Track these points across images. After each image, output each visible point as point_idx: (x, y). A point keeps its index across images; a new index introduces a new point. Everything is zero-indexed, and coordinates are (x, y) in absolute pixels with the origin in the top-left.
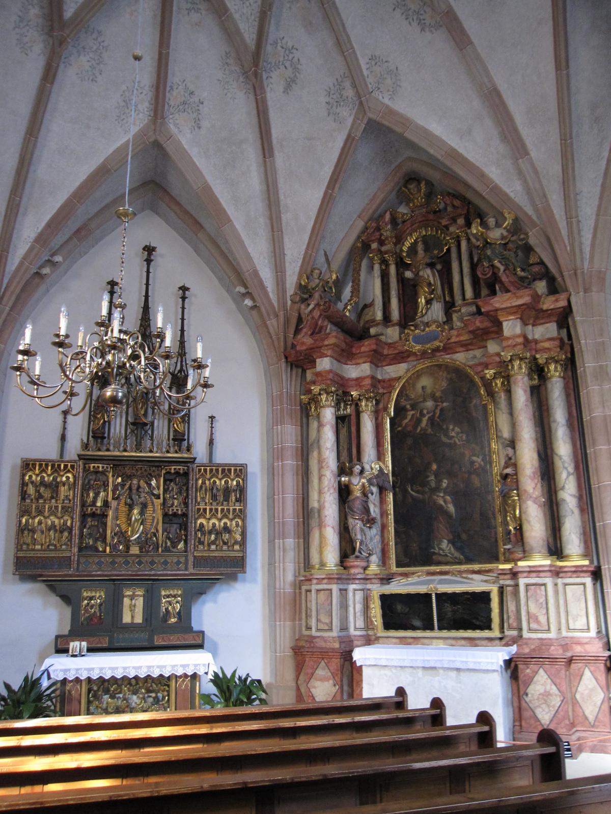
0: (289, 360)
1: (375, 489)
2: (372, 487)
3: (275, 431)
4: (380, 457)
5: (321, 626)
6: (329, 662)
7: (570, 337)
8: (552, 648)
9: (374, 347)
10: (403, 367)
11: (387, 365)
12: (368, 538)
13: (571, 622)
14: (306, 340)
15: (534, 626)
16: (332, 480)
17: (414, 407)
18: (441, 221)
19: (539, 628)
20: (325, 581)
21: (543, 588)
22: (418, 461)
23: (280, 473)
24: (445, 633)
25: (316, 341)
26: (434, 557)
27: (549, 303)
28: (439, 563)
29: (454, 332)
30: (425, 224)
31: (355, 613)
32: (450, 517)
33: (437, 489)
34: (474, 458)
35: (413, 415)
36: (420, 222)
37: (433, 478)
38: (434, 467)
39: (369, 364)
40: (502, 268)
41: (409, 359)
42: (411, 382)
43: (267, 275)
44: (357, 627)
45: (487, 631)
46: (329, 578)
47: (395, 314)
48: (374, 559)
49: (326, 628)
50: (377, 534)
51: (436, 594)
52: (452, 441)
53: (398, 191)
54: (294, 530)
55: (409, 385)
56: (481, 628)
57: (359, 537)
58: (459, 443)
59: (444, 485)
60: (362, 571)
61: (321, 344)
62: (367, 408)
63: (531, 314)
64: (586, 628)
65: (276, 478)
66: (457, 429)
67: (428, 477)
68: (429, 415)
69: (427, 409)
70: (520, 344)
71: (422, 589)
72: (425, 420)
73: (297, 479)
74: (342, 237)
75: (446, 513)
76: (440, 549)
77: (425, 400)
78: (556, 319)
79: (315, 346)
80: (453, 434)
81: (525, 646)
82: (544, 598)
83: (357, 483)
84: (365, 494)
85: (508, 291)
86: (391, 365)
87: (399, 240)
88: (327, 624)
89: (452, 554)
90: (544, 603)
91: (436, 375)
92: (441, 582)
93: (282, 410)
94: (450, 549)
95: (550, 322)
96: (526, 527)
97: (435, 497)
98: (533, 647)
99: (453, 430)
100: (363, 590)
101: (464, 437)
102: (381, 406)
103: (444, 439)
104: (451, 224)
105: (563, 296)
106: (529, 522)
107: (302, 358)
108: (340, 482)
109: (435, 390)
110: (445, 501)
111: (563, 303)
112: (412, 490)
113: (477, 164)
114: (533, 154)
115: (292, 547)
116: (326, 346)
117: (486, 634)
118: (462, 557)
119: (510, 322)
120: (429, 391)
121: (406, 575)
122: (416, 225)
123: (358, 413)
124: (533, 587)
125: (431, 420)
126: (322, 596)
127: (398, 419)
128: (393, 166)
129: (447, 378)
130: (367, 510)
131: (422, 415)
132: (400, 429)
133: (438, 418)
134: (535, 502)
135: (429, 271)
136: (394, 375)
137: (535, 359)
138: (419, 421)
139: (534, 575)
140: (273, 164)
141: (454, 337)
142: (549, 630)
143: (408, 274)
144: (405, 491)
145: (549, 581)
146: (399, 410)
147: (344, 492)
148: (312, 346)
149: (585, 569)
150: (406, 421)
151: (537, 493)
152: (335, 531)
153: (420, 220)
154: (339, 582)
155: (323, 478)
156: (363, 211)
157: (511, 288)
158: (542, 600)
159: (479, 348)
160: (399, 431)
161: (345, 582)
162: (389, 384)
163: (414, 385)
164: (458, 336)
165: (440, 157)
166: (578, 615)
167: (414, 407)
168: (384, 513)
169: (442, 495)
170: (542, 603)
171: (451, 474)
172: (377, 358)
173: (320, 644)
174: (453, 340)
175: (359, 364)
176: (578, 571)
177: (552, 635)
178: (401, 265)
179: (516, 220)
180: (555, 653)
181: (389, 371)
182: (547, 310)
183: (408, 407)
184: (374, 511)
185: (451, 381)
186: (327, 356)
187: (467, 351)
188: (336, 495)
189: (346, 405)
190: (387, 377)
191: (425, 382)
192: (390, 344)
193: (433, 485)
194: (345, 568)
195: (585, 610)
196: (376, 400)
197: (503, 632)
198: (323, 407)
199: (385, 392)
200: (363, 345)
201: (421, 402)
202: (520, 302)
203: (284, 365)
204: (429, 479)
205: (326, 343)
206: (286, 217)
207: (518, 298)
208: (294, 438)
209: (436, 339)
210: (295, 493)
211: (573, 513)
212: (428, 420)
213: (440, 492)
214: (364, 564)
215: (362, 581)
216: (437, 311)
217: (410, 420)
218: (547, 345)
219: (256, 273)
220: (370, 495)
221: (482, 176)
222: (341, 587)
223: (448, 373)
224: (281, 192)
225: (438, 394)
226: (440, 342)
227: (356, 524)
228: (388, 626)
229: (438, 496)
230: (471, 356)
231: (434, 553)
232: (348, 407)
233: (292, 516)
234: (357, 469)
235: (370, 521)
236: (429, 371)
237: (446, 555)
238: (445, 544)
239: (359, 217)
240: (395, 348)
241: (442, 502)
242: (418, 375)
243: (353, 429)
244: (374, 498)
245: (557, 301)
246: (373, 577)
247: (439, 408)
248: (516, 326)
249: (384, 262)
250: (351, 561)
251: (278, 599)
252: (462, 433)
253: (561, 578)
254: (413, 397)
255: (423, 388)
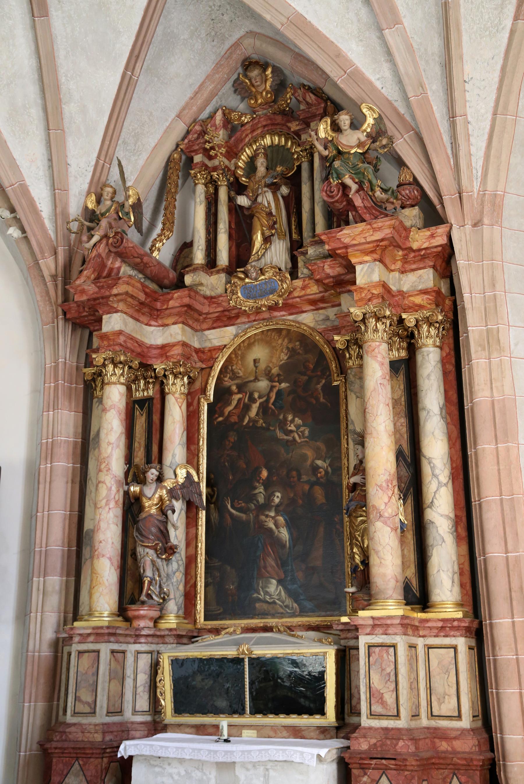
0: (68, 316)
1: (179, 505)
2: (174, 502)
3: (45, 418)
4: (192, 459)
5: (80, 708)
6: (84, 765)
7: (452, 290)
8: (401, 743)
9: (186, 300)
10: (231, 330)
11: (209, 329)
12: (168, 576)
13: (435, 704)
14: (85, 285)
15: (377, 708)
16: (114, 489)
17: (241, 388)
18: (289, 125)
19: (384, 712)
20: (91, 638)
21: (392, 649)
22: (242, 464)
23: (48, 479)
24: (259, 719)
25: (100, 288)
26: (257, 605)
27: (420, 239)
28: (264, 615)
29: (298, 283)
30: (271, 128)
31: (135, 687)
32: (283, 546)
33: (267, 506)
34: (319, 463)
35: (240, 400)
36: (264, 126)
37: (261, 489)
38: (265, 474)
39: (180, 325)
40: (354, 187)
41: (239, 321)
42: (240, 353)
43: (41, 194)
44: (138, 708)
45: (318, 716)
46: (97, 634)
47: (223, 257)
48: (173, 607)
49: (87, 709)
50: (178, 570)
51: (250, 659)
52: (290, 438)
53: (235, 82)
54: (63, 563)
55: (236, 357)
56: (311, 713)
57: (149, 573)
58: (299, 441)
59: (277, 500)
60: (151, 624)
61: (107, 293)
62: (177, 388)
63: (392, 249)
64: (456, 714)
65: (41, 486)
66: (298, 421)
67: (255, 488)
68: (261, 400)
69: (259, 392)
70: (378, 296)
71: (231, 652)
72: (255, 408)
73: (72, 488)
74: (153, 145)
75: (277, 542)
76: (266, 593)
77: (256, 379)
78: (432, 264)
79: (99, 295)
80: (292, 428)
81: (362, 740)
82: (393, 667)
83: (152, 496)
84: (162, 511)
85: (363, 220)
86: (214, 328)
87: (233, 153)
88: (88, 704)
89: (283, 602)
90: (393, 673)
91: (274, 344)
92: (258, 642)
93: (56, 388)
94: (280, 591)
95: (424, 268)
96: (374, 560)
97: (263, 518)
98: (373, 741)
99: (292, 421)
100: (151, 652)
101: (307, 433)
102: (198, 385)
103: (280, 435)
104: (304, 129)
105: (441, 230)
106: (377, 553)
107: (85, 314)
108: (126, 493)
109: (271, 365)
110: (276, 525)
111: (441, 240)
112: (233, 507)
113: (332, 38)
114: (407, 22)
115: (57, 588)
116: (116, 295)
117: (316, 720)
118: (295, 605)
119: (366, 266)
120: (262, 366)
121: (217, 631)
122: (259, 131)
123: (163, 395)
124: (377, 650)
125: (264, 409)
126: (86, 661)
127: (219, 405)
128: (227, 46)
129: (288, 348)
130: (164, 535)
131: (252, 400)
132: (221, 419)
133: (273, 404)
134: (385, 523)
135: (270, 196)
136: (217, 343)
137: (401, 321)
138: (247, 408)
139: (379, 630)
140: (48, 26)
141: (299, 289)
142: (398, 716)
143: (243, 201)
144: (221, 509)
145: (401, 641)
146: (222, 393)
147: (132, 507)
148: (94, 296)
149: (456, 624)
150: (230, 408)
151: (390, 511)
152: (112, 564)
153: (264, 123)
154: (112, 639)
155: (100, 485)
156: (184, 109)
157: (367, 216)
158: (390, 669)
159: (333, 306)
160: (220, 422)
161: (121, 639)
162: (208, 355)
163: (243, 357)
164: (303, 288)
165: (279, 26)
166: (445, 694)
167: (241, 388)
168: (191, 540)
169: (272, 514)
170: (389, 674)
171: (286, 485)
172: (190, 315)
173: (76, 735)
174: (296, 294)
175: (167, 325)
176: (446, 627)
177: (401, 724)
178: (237, 188)
179: (379, 120)
180: (404, 750)
181: (210, 337)
182: (420, 250)
183: (234, 388)
184: (177, 536)
185: (292, 352)
186: (117, 311)
187: (317, 309)
188: (119, 512)
189: (147, 383)
190: (208, 345)
191: (259, 352)
192: (212, 298)
193: (261, 499)
194: (128, 620)
195: (455, 686)
196: (189, 377)
197: (343, 719)
198: (108, 384)
199: (204, 366)
200: (172, 298)
201: (251, 381)
202: (378, 236)
203: (61, 323)
204: (257, 491)
205: (115, 291)
206: (70, 110)
207: (375, 230)
208: (71, 430)
209: (272, 291)
210: (68, 509)
211: (444, 541)
212: (259, 408)
213: (270, 510)
214: (155, 614)
215: (150, 639)
216: (278, 253)
217: (236, 407)
218: (418, 300)
219: (24, 189)
220: (170, 512)
221: (338, 56)
222: (116, 647)
223: (290, 341)
224: (62, 71)
225: (275, 371)
226: (280, 296)
227: (147, 555)
228: (180, 708)
229: (267, 516)
230: (322, 317)
231: (259, 600)
232: (151, 386)
233: (60, 543)
234: (152, 474)
235: (169, 550)
236: (265, 338)
237: (274, 603)
238: (273, 587)
239: (178, 116)
240: (219, 305)
241: (271, 525)
242: (249, 343)
243: (156, 418)
244: (178, 516)
245: (432, 236)
246: (167, 633)
247: (275, 390)
248: (373, 271)
249: (212, 184)
250: (134, 610)
251: (29, 668)
252: (304, 425)
253: (423, 636)
254: (241, 374)
255: (255, 361)
